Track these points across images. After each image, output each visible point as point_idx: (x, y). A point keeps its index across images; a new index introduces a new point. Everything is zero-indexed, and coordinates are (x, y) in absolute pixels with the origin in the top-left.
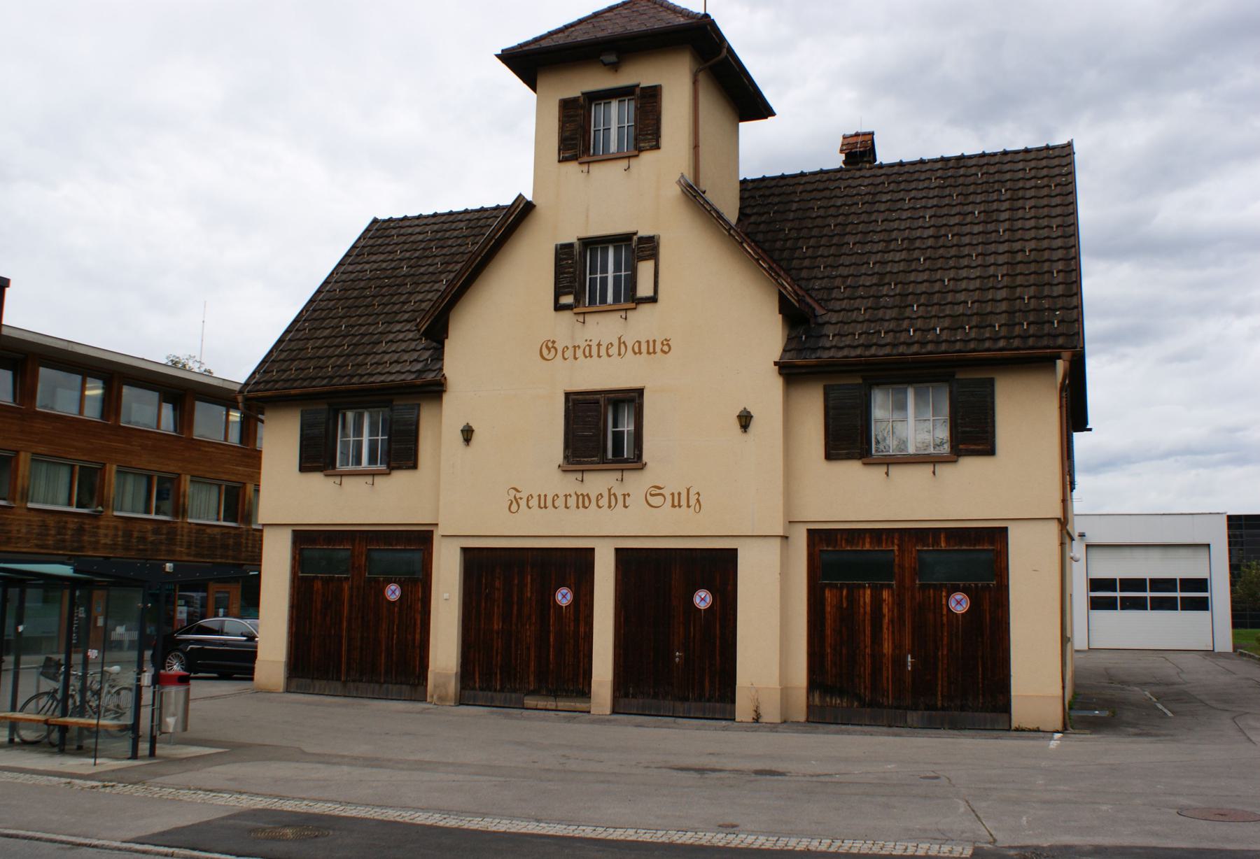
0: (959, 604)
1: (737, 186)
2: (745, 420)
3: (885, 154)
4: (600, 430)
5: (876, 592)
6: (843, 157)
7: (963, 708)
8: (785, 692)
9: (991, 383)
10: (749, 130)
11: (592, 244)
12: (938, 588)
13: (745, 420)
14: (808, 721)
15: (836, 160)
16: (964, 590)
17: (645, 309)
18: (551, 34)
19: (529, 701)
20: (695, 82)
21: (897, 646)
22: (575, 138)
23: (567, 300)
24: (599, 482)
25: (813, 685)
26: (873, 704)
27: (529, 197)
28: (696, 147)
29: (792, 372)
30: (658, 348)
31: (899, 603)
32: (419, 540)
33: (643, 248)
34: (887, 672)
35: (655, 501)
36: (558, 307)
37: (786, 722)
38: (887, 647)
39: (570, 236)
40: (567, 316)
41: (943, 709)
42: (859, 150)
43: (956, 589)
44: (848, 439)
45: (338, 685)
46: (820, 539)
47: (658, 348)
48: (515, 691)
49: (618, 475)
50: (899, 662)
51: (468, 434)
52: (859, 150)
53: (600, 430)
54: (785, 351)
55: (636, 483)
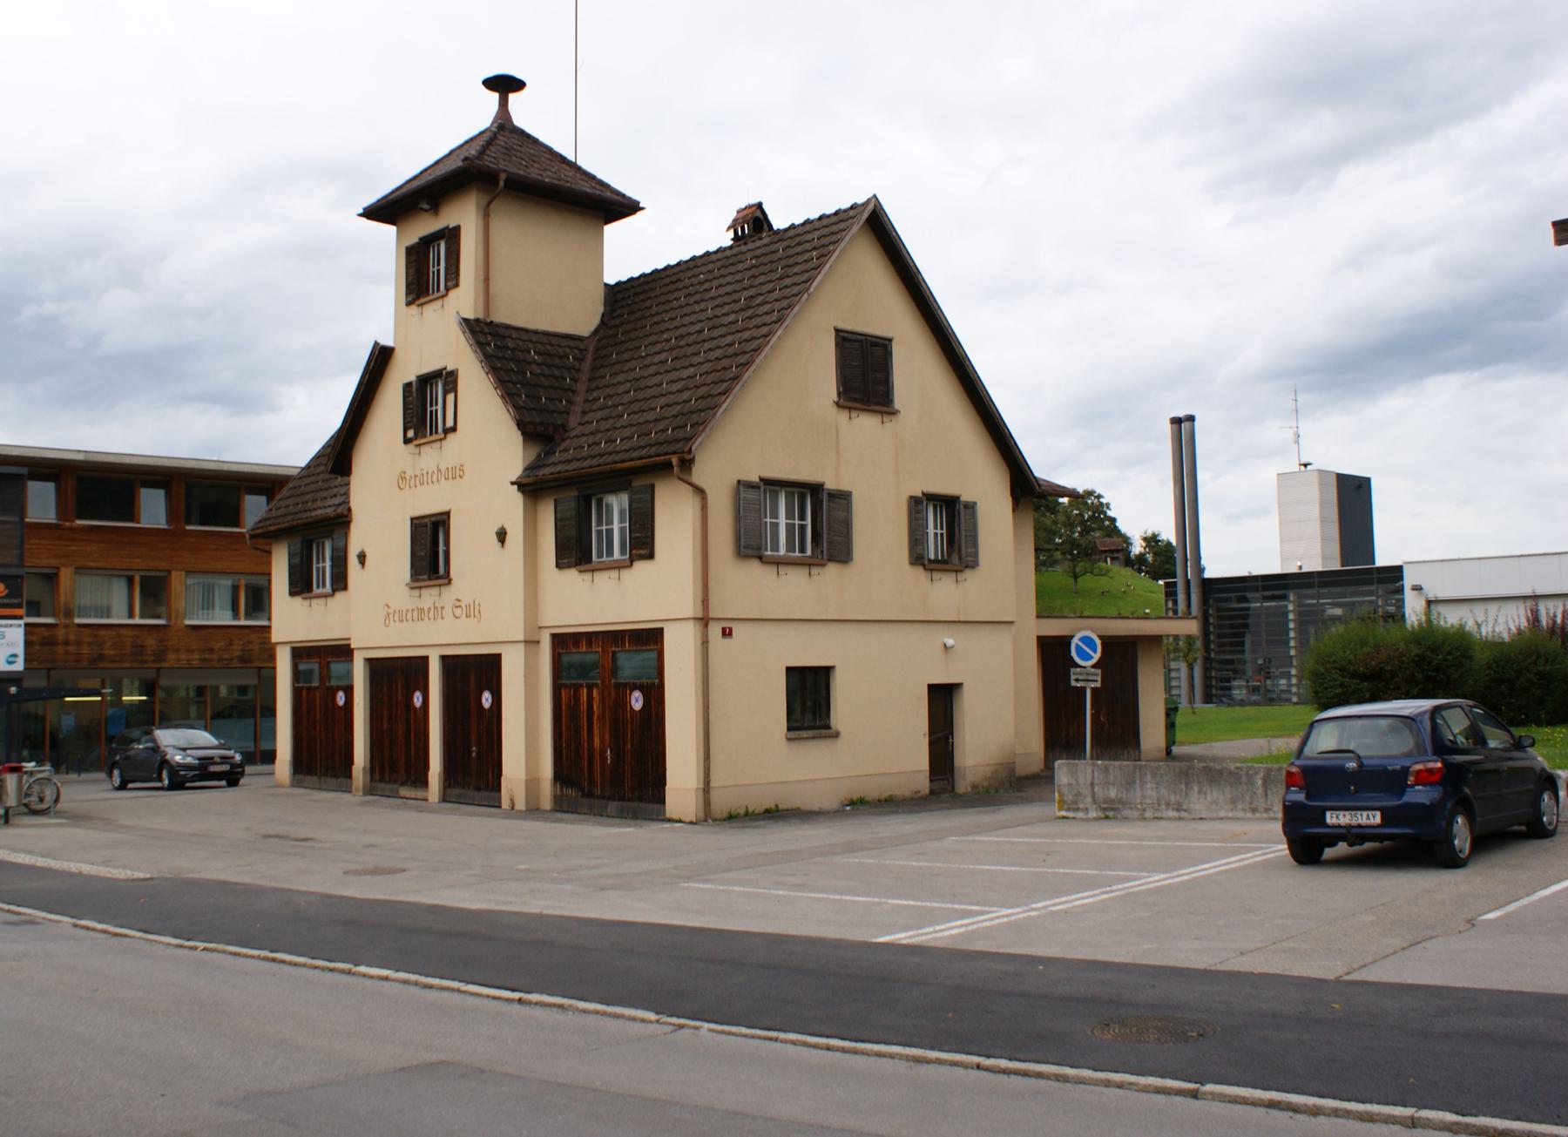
0: (637, 701)
1: (600, 294)
2: (502, 536)
3: (779, 221)
4: (430, 548)
5: (590, 688)
6: (731, 234)
7: (640, 799)
8: (532, 784)
9: (653, 487)
10: (612, 231)
11: (426, 380)
12: (625, 685)
13: (502, 536)
14: (554, 810)
15: (726, 240)
16: (641, 688)
17: (451, 436)
18: (407, 182)
19: (404, 791)
20: (486, 216)
21: (602, 741)
22: (423, 277)
23: (411, 434)
24: (429, 597)
25: (560, 776)
26: (590, 795)
27: (388, 341)
28: (487, 279)
29: (532, 487)
30: (456, 473)
31: (603, 702)
32: (344, 651)
33: (449, 379)
34: (597, 766)
35: (458, 612)
36: (407, 441)
37: (533, 811)
38: (597, 740)
39: (411, 378)
40: (411, 447)
41: (629, 800)
42: (753, 221)
43: (635, 687)
44: (575, 550)
45: (315, 778)
46: (562, 642)
47: (456, 473)
48: (395, 782)
49: (435, 591)
50: (603, 753)
51: (362, 558)
52: (753, 221)
53: (430, 548)
54: (526, 469)
55: (450, 594)
